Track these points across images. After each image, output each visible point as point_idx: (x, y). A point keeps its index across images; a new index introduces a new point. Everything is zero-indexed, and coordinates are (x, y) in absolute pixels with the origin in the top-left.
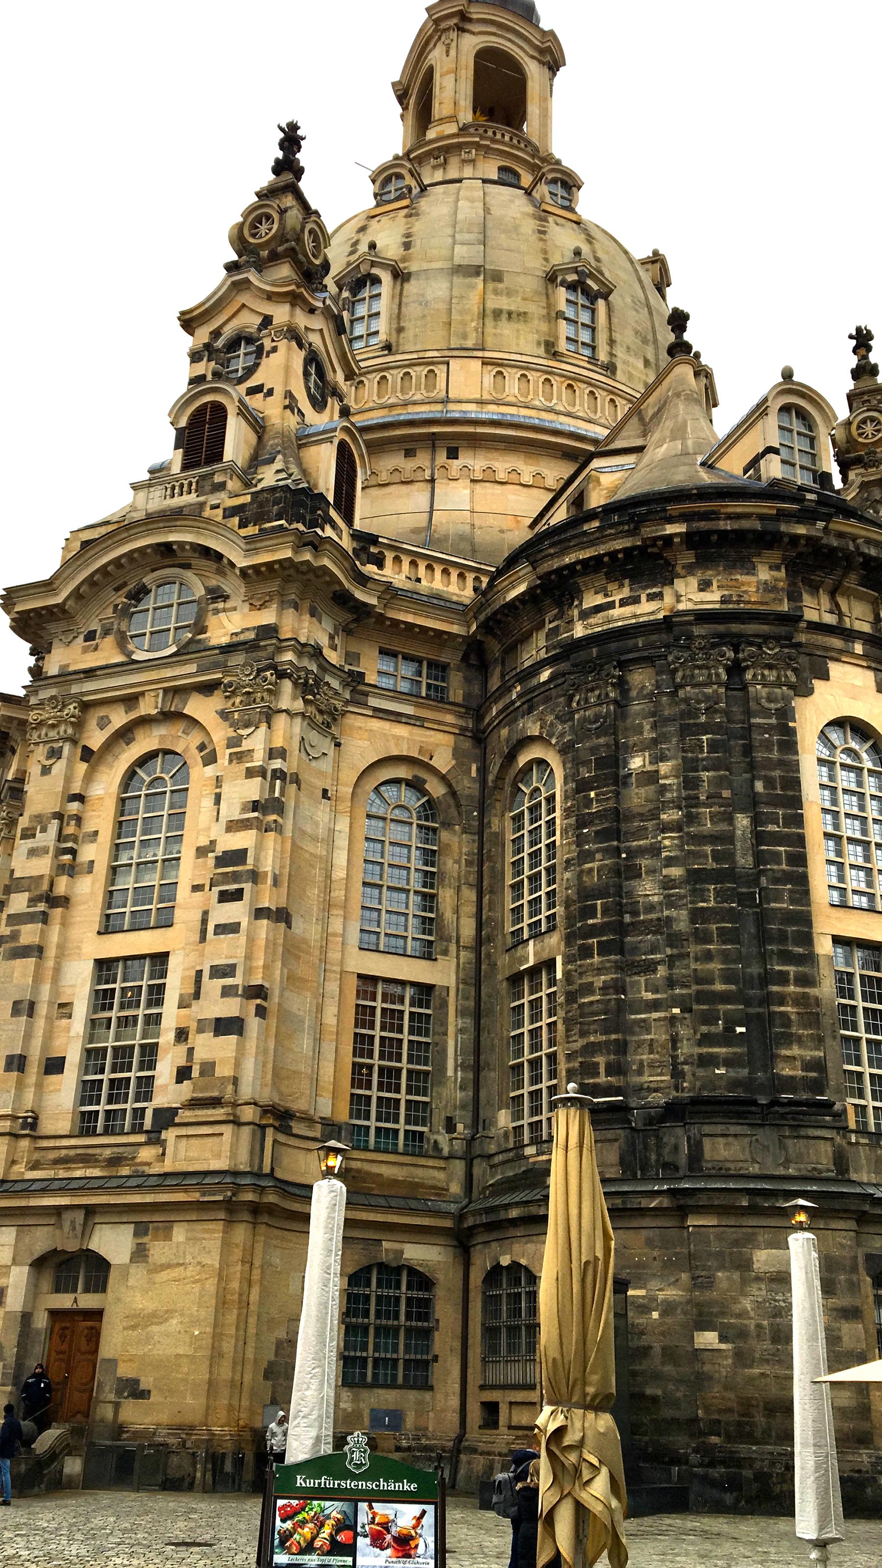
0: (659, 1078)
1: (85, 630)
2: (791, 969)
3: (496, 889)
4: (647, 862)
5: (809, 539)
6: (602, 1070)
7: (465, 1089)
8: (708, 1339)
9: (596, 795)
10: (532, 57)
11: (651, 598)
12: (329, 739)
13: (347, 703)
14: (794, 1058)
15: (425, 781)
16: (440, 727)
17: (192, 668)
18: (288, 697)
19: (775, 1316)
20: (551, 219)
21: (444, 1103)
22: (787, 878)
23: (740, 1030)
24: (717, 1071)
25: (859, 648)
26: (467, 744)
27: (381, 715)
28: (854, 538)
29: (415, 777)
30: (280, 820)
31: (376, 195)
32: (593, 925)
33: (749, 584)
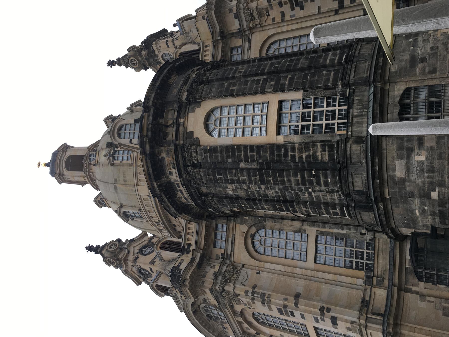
1: (223, 329)
2: (290, 153)
5: (150, 142)
8: (434, 195)
11: (179, 187)
13: (230, 261)
14: (321, 155)
16: (234, 229)
17: (227, 310)
18: (229, 288)
19: (423, 171)
20: (99, 161)
21: (356, 235)
22: (258, 153)
23: (313, 173)
25: (182, 120)
26: (238, 220)
28: (148, 125)
33: (168, 160)
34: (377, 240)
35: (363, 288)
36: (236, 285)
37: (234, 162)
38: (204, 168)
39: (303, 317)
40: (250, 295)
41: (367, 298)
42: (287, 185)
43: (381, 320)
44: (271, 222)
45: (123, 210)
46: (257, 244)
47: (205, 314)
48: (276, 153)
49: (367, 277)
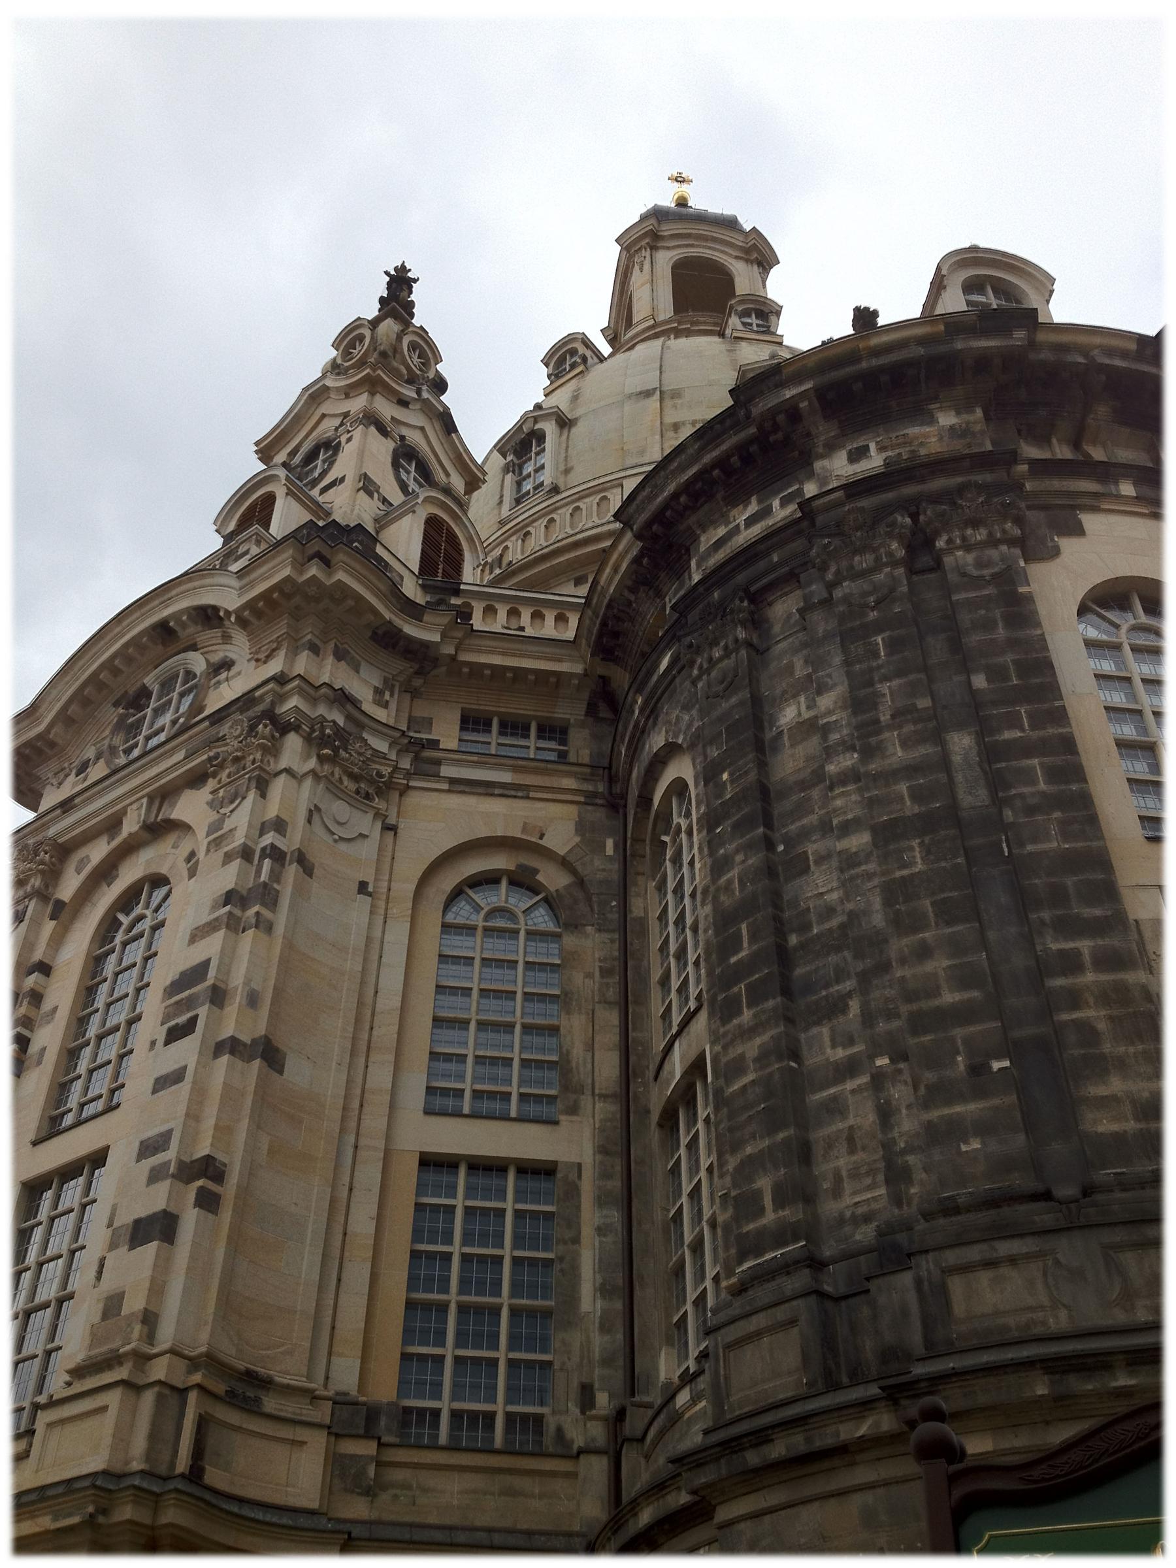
2: (1085, 946)
3: (643, 999)
4: (815, 846)
5: (1012, 360)
6: (768, 1201)
9: (731, 775)
10: (737, 258)
12: (370, 816)
13: (408, 775)
14: (1115, 1098)
15: (536, 871)
16: (553, 795)
17: (180, 755)
23: (996, 1065)
24: (964, 1148)
26: (598, 815)
27: (462, 788)
29: (519, 866)
30: (266, 913)
31: (549, 376)
33: (926, 436)
35: (316, 1385)
36: (308, 782)
37: (975, 701)
38: (910, 583)
39: (163, 1083)
40: (269, 839)
41: (270, 1404)
42: (899, 945)
43: (172, 1465)
45: (549, 428)
46: (487, 899)
47: (151, 681)
48: (1070, 881)
49: (372, 1413)
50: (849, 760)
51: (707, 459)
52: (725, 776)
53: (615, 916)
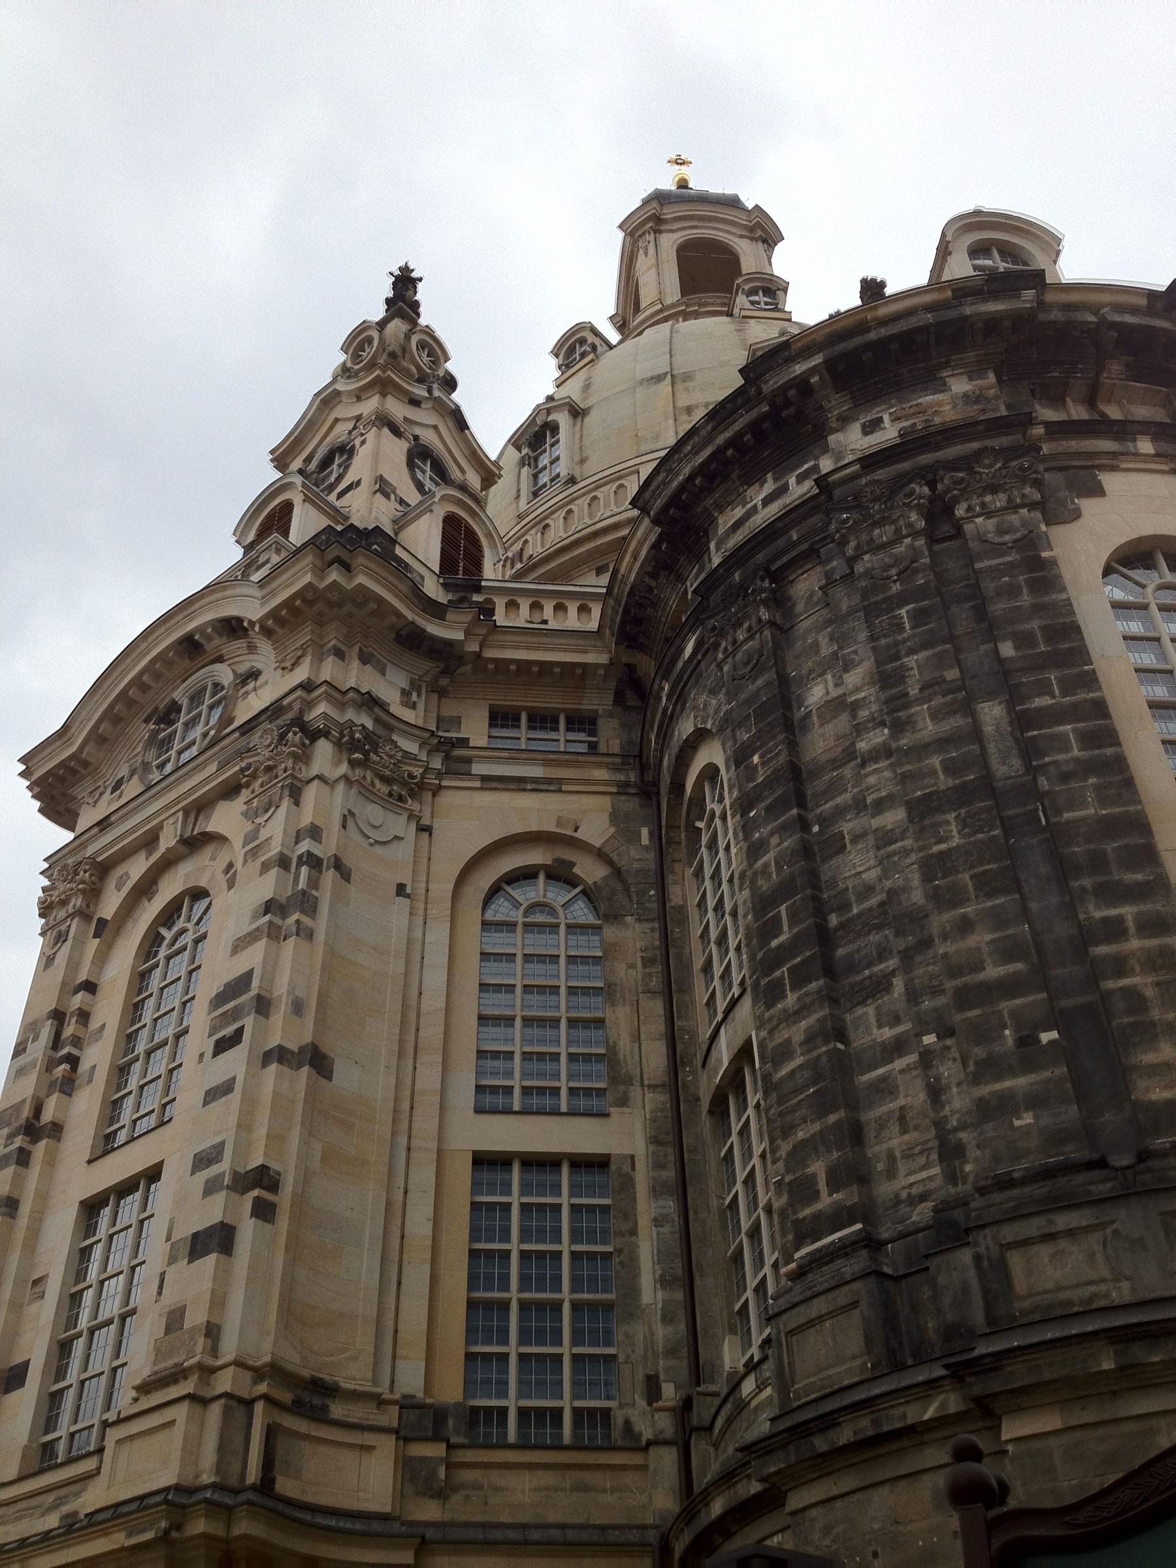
0: (924, 1175)
1: (112, 782)
2: (1128, 912)
3: (686, 987)
4: (851, 825)
5: (1020, 320)
6: (822, 1185)
7: (671, 1321)
9: (761, 757)
10: (741, 236)
12: (405, 816)
13: (440, 775)
15: (573, 864)
16: (587, 788)
17: (213, 768)
21: (640, 1352)
22: (1087, 768)
23: (1046, 1037)
24: (1017, 1123)
26: (631, 804)
27: (494, 785)
29: (556, 860)
30: (306, 920)
31: (560, 367)
32: (781, 946)
33: (940, 404)
34: (636, 1459)
35: (383, 1389)
38: (932, 554)
39: (212, 1095)
40: (305, 846)
41: (338, 1410)
42: (940, 921)
43: (243, 1476)
44: (639, 945)
45: (562, 419)
46: (526, 894)
47: (180, 694)
48: (1110, 847)
49: (439, 1415)
50: (878, 737)
51: (721, 439)
52: (756, 759)
53: (654, 906)
